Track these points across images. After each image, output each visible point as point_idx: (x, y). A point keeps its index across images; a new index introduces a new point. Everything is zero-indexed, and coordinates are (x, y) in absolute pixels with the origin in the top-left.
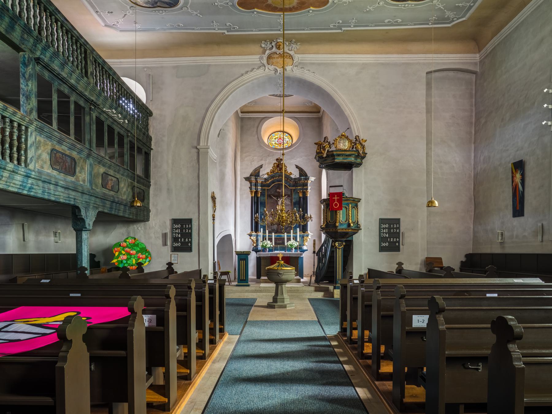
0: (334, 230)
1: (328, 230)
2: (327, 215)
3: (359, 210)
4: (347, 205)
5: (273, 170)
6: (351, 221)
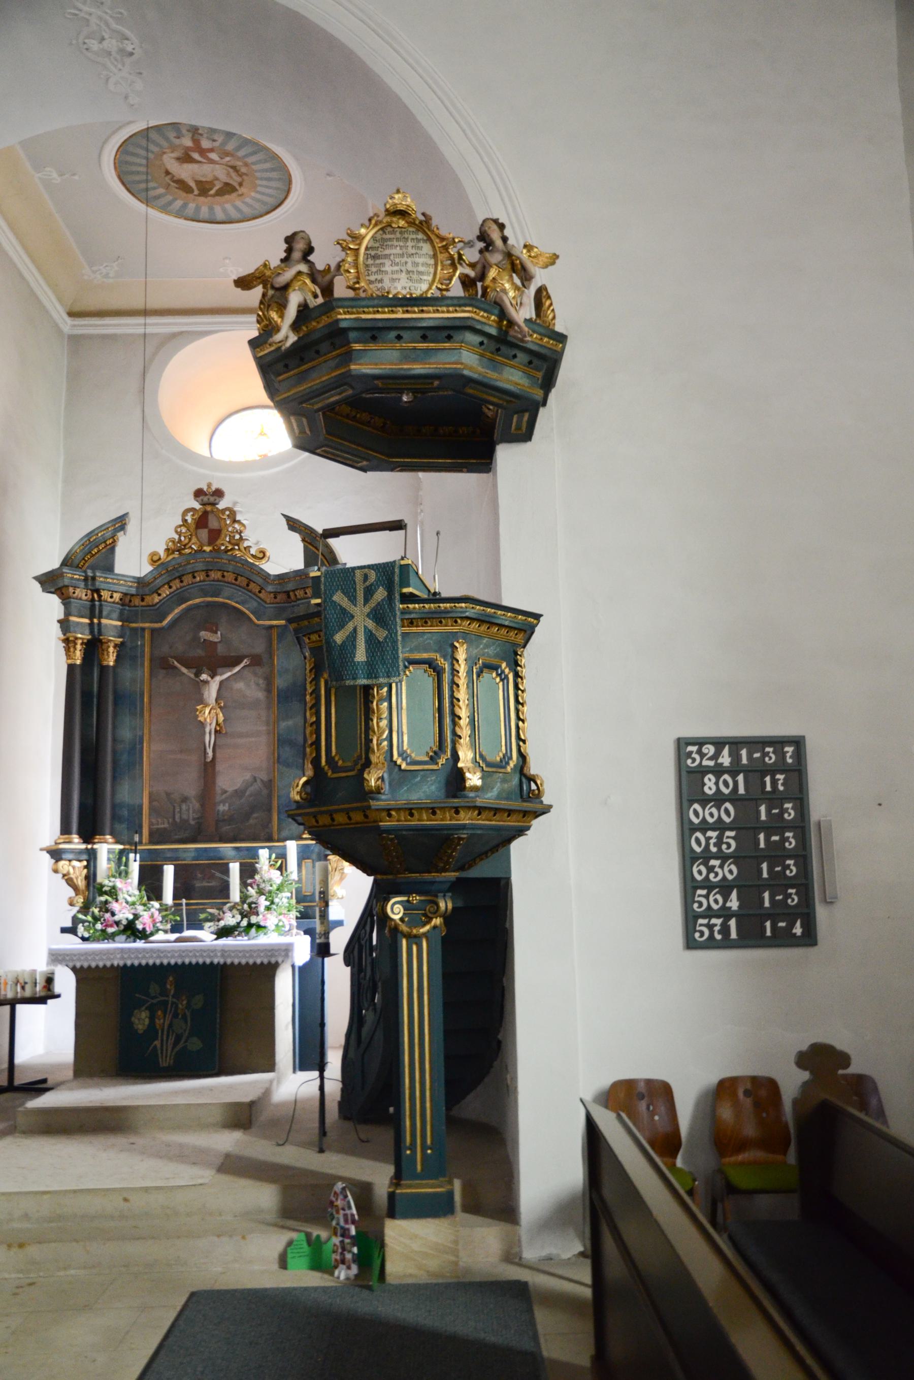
0: (358, 817)
1: (324, 820)
2: (318, 722)
3: (525, 684)
4: (439, 650)
5: (180, 541)
6: (470, 755)
